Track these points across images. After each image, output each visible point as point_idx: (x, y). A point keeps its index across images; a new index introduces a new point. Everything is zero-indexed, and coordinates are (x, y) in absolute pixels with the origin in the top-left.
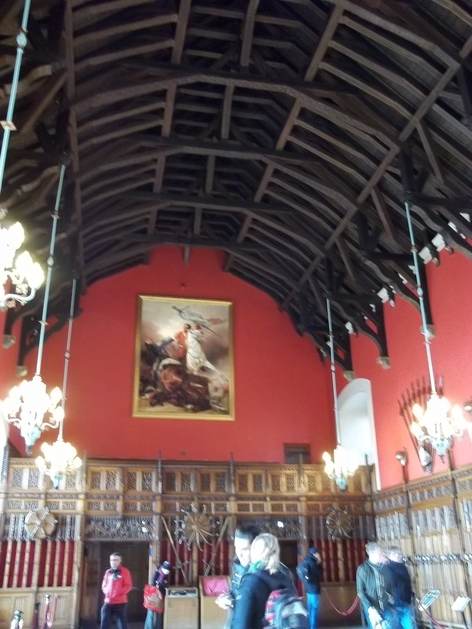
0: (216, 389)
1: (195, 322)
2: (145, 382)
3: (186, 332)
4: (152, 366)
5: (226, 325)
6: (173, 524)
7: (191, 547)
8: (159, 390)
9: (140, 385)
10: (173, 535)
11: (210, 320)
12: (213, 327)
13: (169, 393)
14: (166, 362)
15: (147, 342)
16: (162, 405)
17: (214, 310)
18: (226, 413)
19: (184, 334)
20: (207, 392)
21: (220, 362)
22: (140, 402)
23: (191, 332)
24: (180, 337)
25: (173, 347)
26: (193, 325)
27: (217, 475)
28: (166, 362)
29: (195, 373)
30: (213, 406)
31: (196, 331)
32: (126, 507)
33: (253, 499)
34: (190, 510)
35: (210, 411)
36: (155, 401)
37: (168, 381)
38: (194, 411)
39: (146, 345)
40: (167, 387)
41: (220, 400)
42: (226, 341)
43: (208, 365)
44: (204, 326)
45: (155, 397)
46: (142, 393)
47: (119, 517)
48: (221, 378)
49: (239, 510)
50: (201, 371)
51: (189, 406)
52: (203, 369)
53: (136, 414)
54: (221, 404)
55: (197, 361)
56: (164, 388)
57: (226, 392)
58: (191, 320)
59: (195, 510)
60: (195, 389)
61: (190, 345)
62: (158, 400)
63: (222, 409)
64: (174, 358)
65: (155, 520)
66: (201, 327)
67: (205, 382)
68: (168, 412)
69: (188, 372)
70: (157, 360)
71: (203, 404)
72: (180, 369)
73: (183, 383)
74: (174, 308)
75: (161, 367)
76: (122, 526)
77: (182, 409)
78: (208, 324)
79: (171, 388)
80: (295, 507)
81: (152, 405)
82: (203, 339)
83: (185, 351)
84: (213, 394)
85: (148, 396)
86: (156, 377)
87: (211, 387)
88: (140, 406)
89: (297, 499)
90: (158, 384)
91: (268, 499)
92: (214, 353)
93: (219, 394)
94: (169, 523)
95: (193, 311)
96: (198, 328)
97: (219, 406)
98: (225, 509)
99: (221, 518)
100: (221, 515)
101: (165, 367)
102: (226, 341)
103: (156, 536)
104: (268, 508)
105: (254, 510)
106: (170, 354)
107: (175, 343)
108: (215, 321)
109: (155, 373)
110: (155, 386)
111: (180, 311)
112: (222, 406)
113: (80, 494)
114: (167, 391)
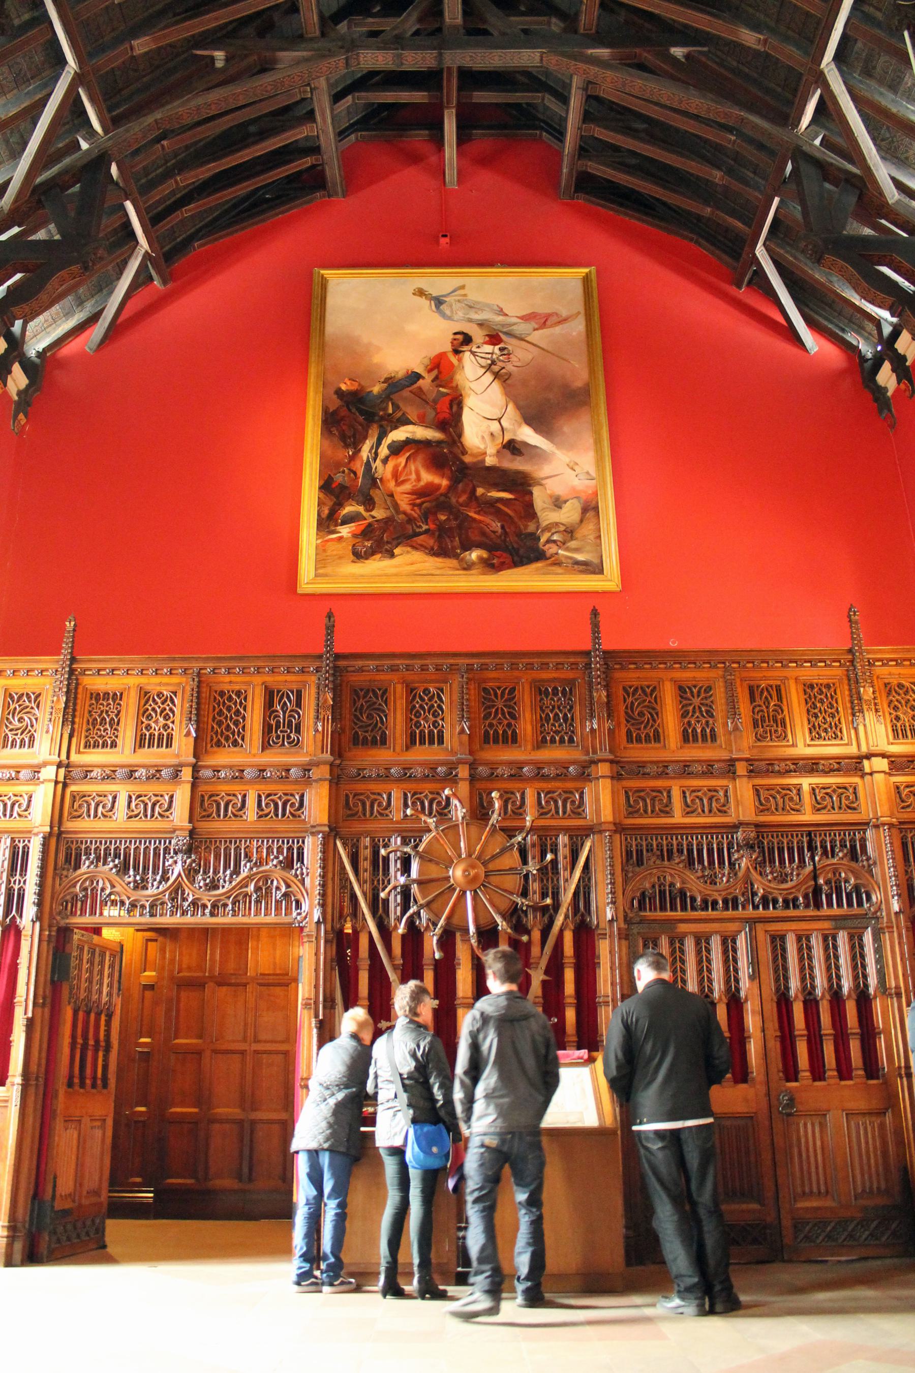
0: (558, 503)
1: (481, 324)
2: (334, 492)
3: (456, 352)
4: (356, 446)
5: (578, 327)
6: (379, 865)
7: (447, 941)
8: (379, 513)
9: (320, 504)
10: (375, 904)
11: (526, 318)
12: (537, 337)
13: (410, 520)
14: (399, 434)
15: (344, 387)
16: (392, 556)
17: (537, 300)
18: (595, 568)
19: (453, 359)
20: (530, 512)
21: (567, 427)
22: (321, 550)
23: (473, 353)
24: (441, 368)
25: (420, 394)
26: (478, 335)
27: (540, 690)
28: (399, 434)
29: (490, 461)
30: (551, 549)
31: (488, 348)
32: (201, 806)
33: (685, 770)
34: (443, 812)
35: (539, 565)
36: (368, 544)
37: (407, 487)
38: (491, 566)
39: (339, 393)
40: (404, 505)
41: (570, 532)
42: (577, 370)
43: (527, 435)
44: (508, 334)
45: (366, 533)
46: (327, 523)
47: (180, 840)
48: (570, 469)
49: (632, 812)
50: (506, 452)
51: (474, 555)
52: (513, 447)
53: (308, 576)
54: (573, 544)
55: (495, 426)
56: (396, 506)
57: (590, 509)
58: (470, 320)
59: (459, 811)
60: (491, 506)
61: (473, 385)
62: (378, 541)
63: (580, 557)
64: (422, 421)
65: (312, 847)
66: (503, 337)
67: (521, 485)
68: (407, 571)
69: (467, 459)
70: (374, 433)
71: (518, 545)
72: (446, 453)
73: (450, 488)
74: (420, 293)
75: (384, 451)
76: (191, 873)
77: (453, 562)
78: (522, 328)
79: (414, 505)
80: (848, 798)
81: (358, 556)
82: (510, 367)
83: (456, 402)
84: (547, 516)
85: (345, 531)
86: (372, 481)
87: (539, 497)
88: (321, 560)
89: (855, 765)
90: (376, 494)
91: (741, 769)
92: (545, 404)
93: (569, 514)
94: (365, 865)
95: (473, 296)
96: (494, 339)
97: (567, 549)
98: (578, 811)
99: (563, 840)
100: (566, 830)
101: (397, 449)
102: (577, 370)
103: (311, 910)
104: (743, 801)
105: (689, 810)
106: (412, 414)
107: (426, 383)
108: (543, 321)
109: (368, 465)
110: (369, 503)
111: (439, 302)
112: (577, 550)
113: (45, 764)
114: (405, 513)
